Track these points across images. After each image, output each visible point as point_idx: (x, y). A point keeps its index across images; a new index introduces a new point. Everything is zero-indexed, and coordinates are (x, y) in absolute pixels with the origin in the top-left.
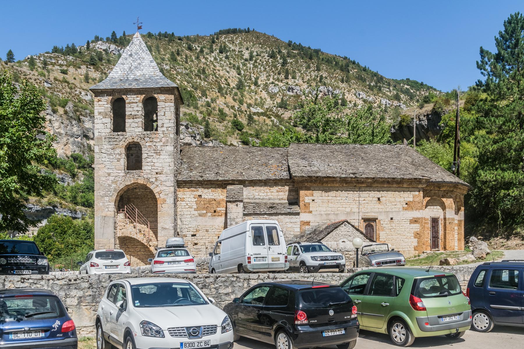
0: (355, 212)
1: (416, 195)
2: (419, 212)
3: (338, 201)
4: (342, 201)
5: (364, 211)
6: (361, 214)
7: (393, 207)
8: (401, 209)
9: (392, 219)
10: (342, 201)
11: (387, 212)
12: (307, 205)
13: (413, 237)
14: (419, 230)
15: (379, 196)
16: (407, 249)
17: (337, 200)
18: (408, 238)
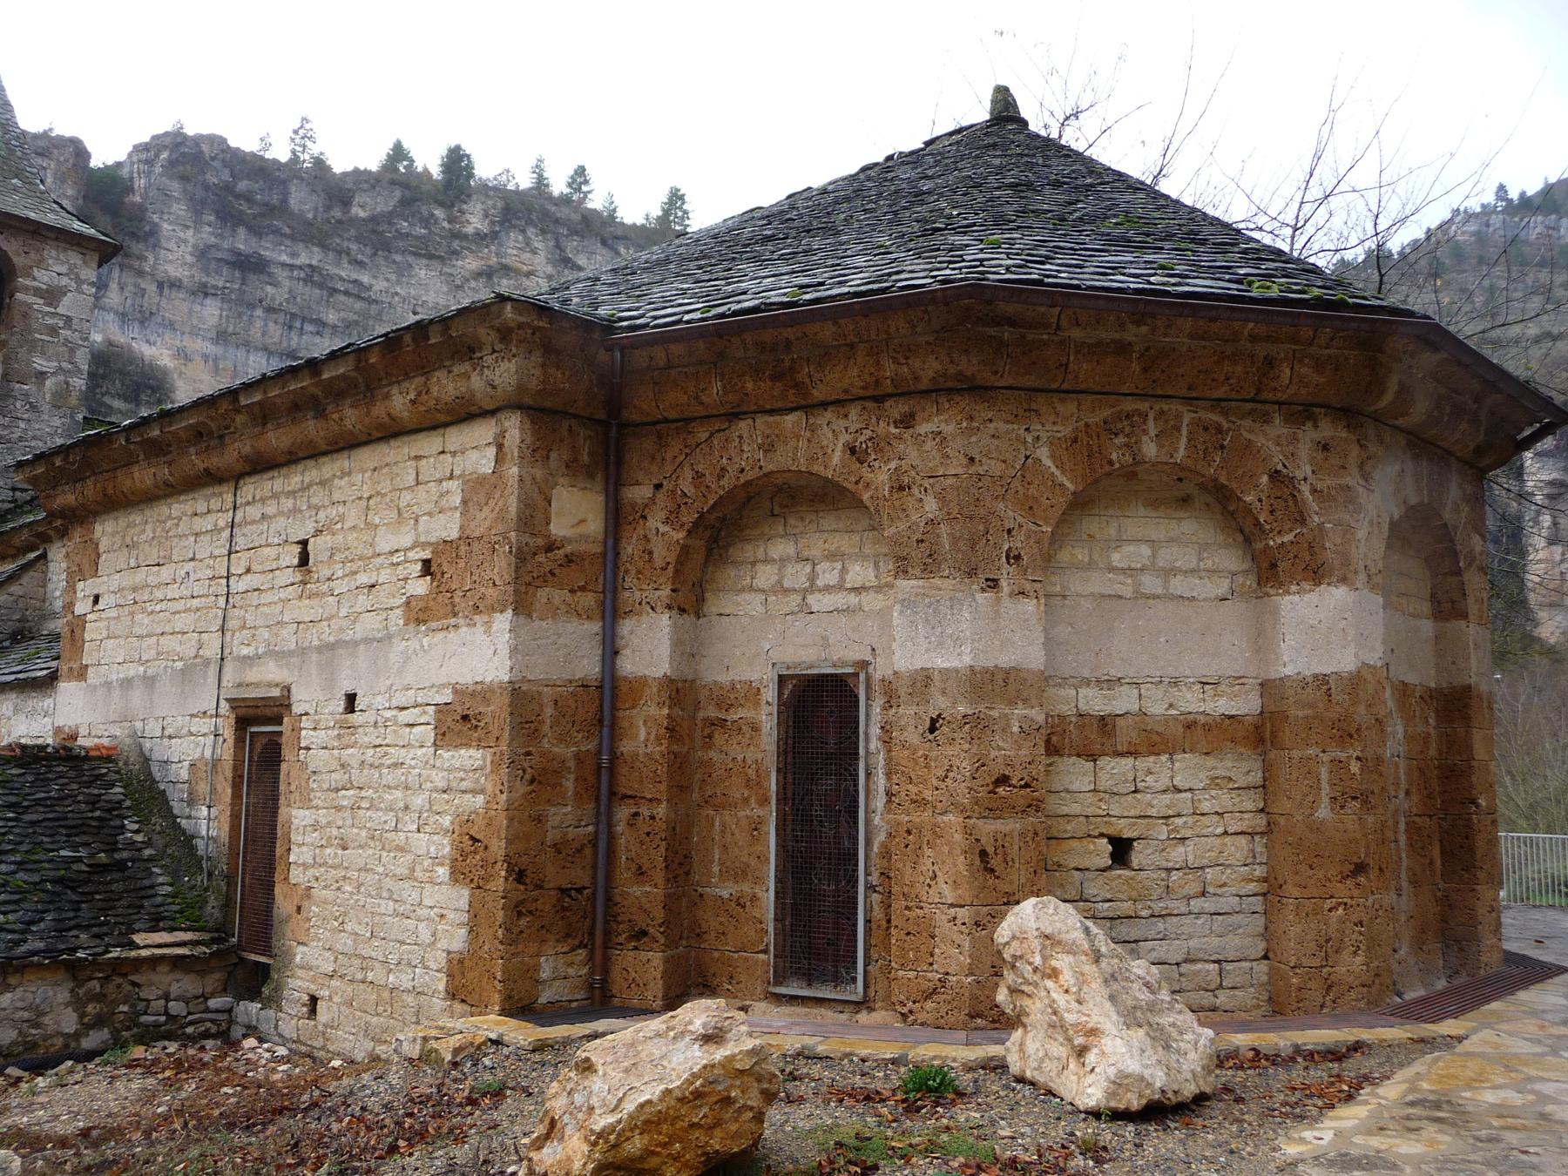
0: (207, 662)
1: (481, 480)
2: (488, 632)
3: (159, 594)
4: (172, 592)
5: (245, 651)
6: (229, 677)
7: (363, 601)
8: (397, 618)
9: (351, 699)
10: (172, 592)
11: (331, 647)
12: (78, 631)
13: (442, 872)
14: (480, 799)
15: (304, 530)
16: (404, 979)
17: (158, 586)
18: (419, 874)
